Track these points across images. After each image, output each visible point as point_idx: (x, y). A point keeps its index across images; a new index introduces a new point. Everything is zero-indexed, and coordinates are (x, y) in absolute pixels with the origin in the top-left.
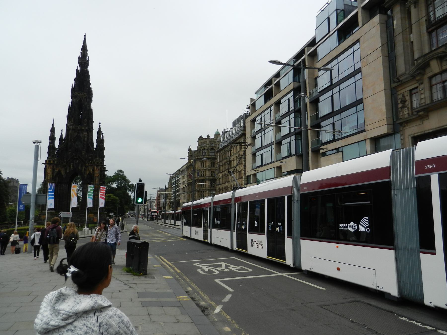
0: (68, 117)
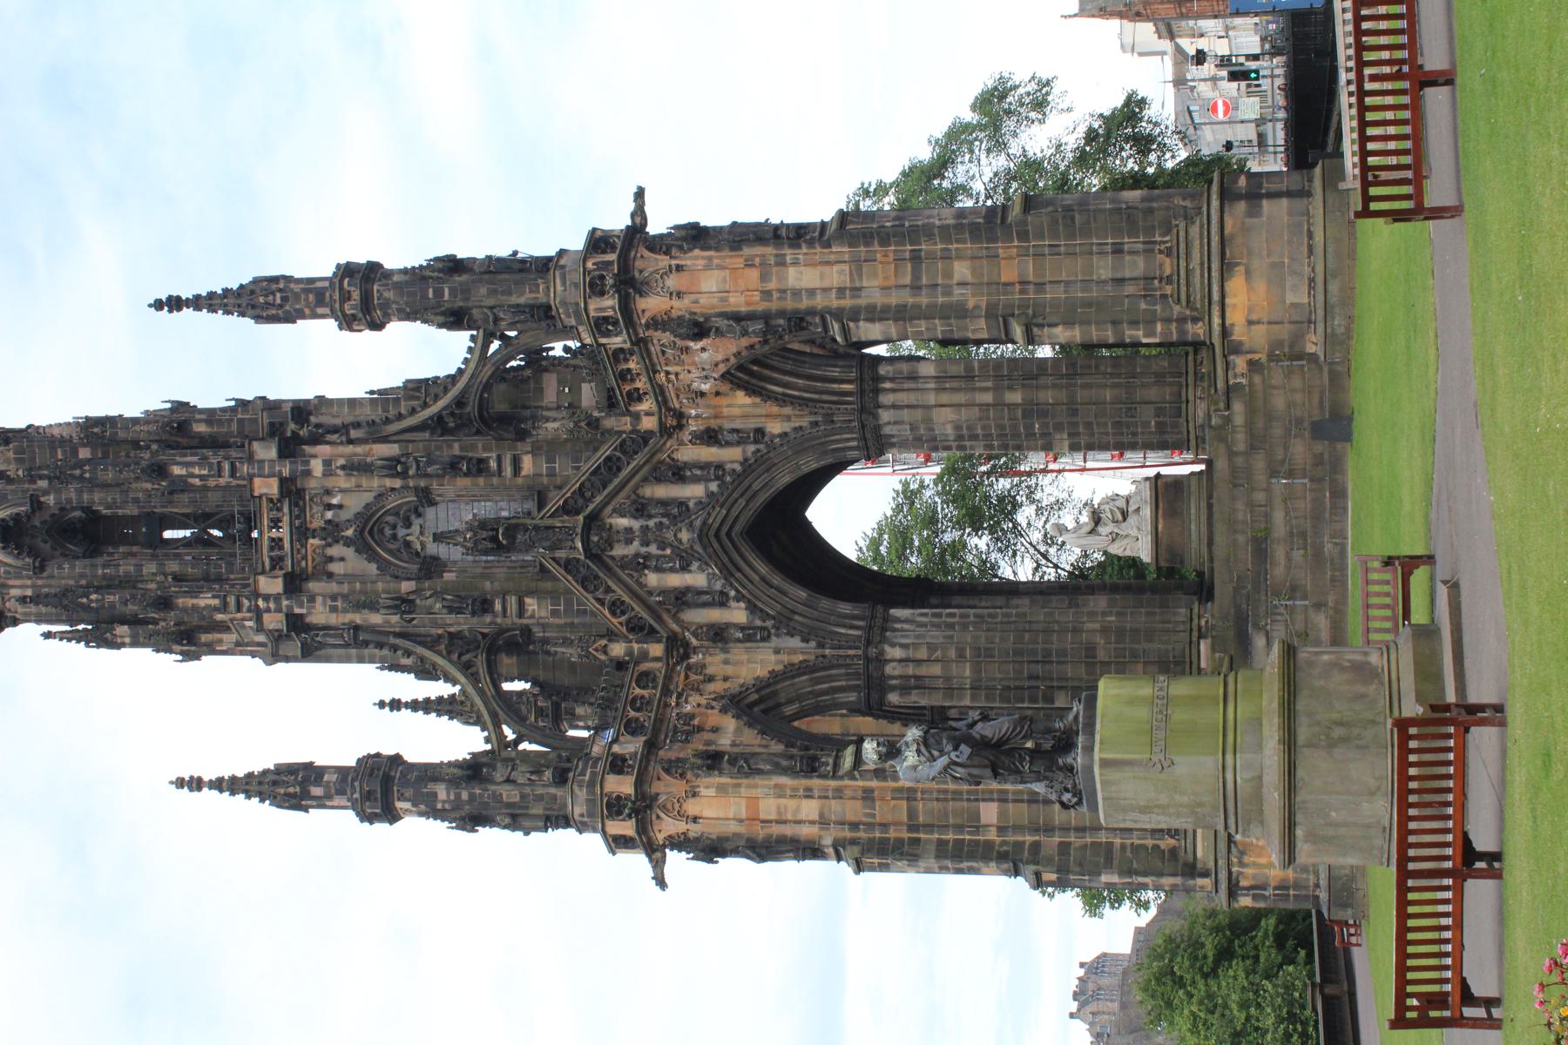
0: (189, 640)
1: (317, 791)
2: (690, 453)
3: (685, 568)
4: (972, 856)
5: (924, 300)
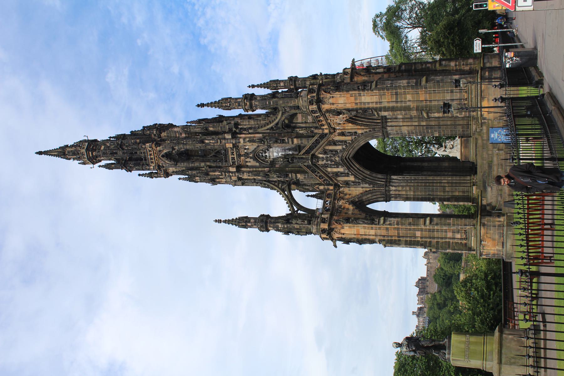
0: (214, 181)
1: (249, 224)
2: (338, 138)
3: (338, 167)
4: (414, 245)
5: (399, 105)
